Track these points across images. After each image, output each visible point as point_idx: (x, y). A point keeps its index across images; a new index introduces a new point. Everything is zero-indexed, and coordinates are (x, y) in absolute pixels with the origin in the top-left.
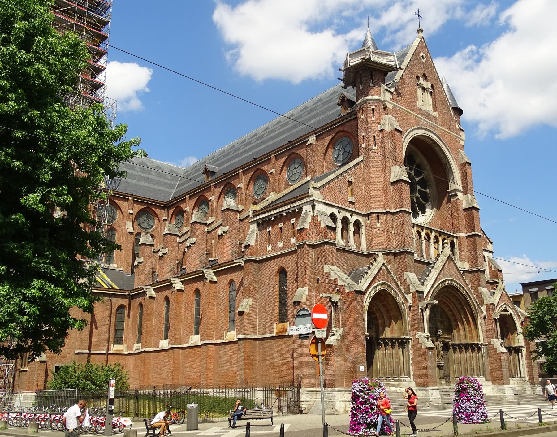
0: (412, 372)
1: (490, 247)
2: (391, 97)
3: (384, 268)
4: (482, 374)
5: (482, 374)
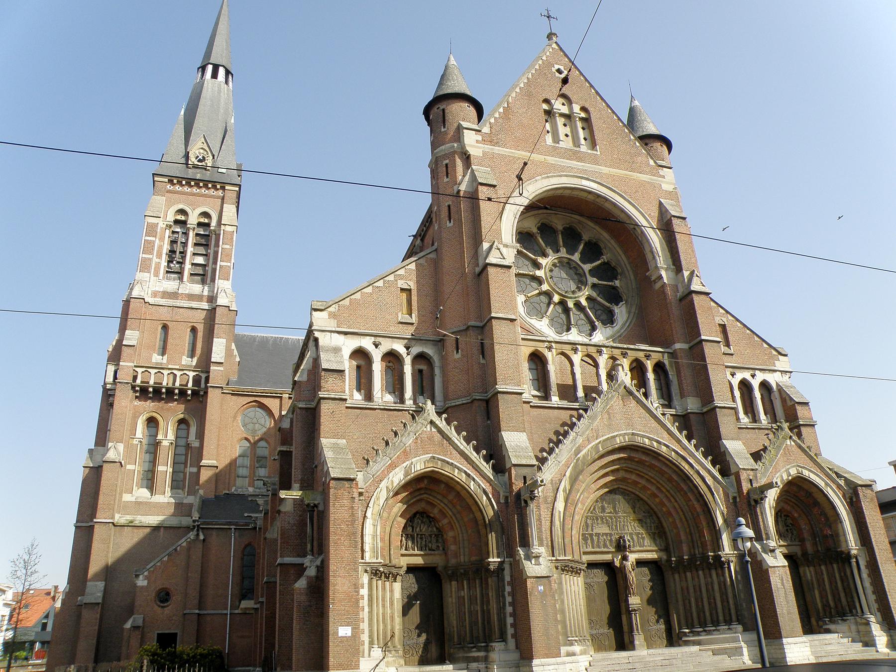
0: (510, 631)
1: (782, 363)
2: (480, 138)
4: (734, 618)
5: (734, 618)
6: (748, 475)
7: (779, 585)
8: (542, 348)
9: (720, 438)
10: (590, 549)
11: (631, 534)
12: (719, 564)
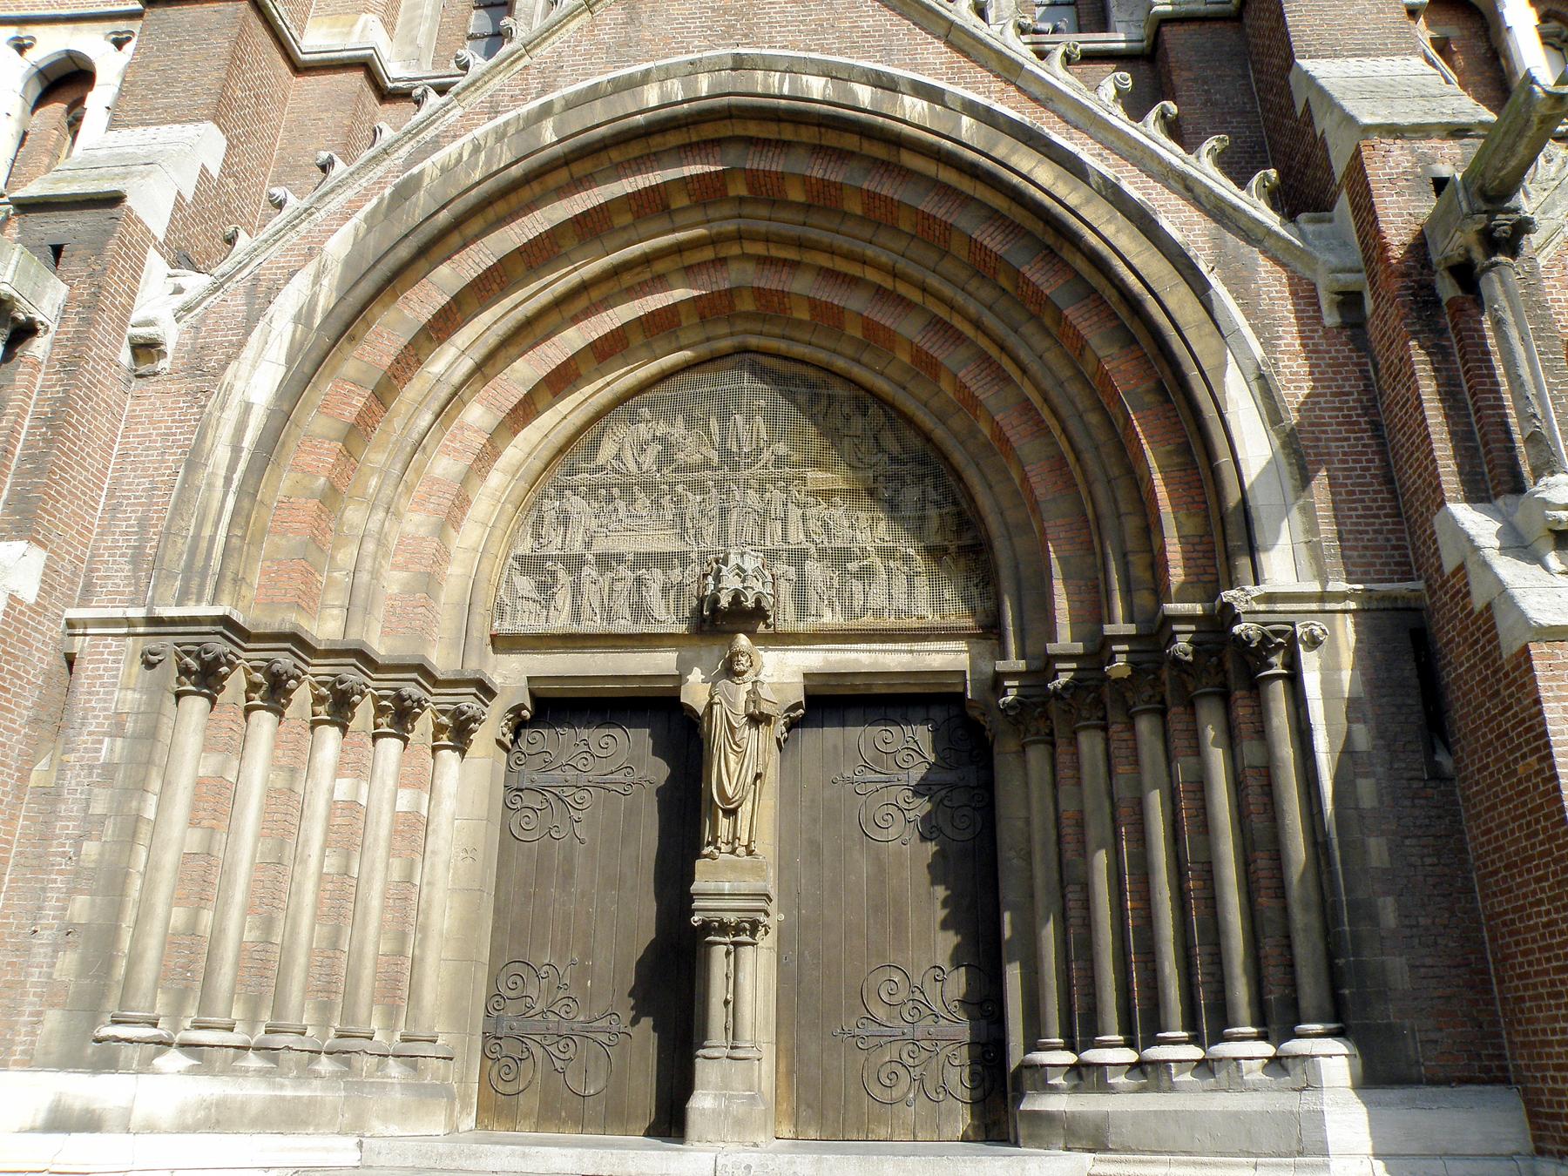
4: (1311, 989)
9: (1289, 58)
10: (560, 622)
11: (798, 557)
12: (1238, 668)
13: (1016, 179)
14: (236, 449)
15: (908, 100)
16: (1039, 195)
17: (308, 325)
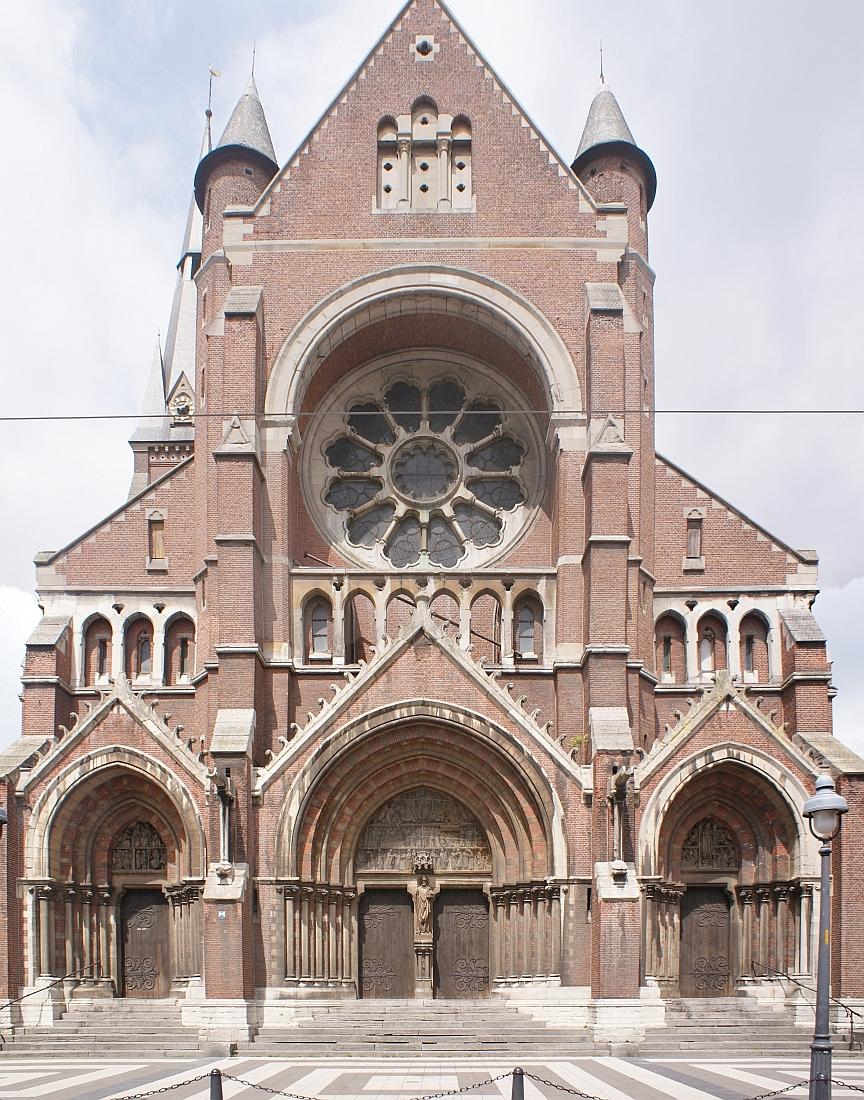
3: (123, 711)
6: (613, 761)
7: (615, 925)
8: (327, 587)
13: (504, 752)
14: (290, 831)
15: (474, 721)
16: (510, 758)
17: (303, 791)
